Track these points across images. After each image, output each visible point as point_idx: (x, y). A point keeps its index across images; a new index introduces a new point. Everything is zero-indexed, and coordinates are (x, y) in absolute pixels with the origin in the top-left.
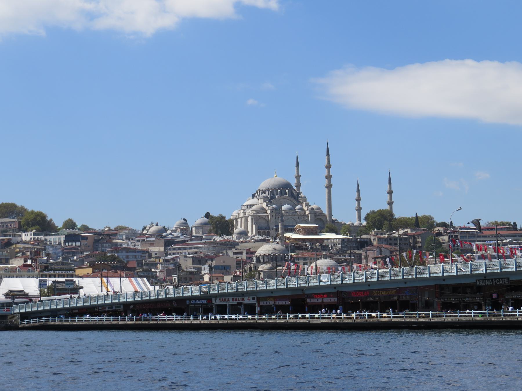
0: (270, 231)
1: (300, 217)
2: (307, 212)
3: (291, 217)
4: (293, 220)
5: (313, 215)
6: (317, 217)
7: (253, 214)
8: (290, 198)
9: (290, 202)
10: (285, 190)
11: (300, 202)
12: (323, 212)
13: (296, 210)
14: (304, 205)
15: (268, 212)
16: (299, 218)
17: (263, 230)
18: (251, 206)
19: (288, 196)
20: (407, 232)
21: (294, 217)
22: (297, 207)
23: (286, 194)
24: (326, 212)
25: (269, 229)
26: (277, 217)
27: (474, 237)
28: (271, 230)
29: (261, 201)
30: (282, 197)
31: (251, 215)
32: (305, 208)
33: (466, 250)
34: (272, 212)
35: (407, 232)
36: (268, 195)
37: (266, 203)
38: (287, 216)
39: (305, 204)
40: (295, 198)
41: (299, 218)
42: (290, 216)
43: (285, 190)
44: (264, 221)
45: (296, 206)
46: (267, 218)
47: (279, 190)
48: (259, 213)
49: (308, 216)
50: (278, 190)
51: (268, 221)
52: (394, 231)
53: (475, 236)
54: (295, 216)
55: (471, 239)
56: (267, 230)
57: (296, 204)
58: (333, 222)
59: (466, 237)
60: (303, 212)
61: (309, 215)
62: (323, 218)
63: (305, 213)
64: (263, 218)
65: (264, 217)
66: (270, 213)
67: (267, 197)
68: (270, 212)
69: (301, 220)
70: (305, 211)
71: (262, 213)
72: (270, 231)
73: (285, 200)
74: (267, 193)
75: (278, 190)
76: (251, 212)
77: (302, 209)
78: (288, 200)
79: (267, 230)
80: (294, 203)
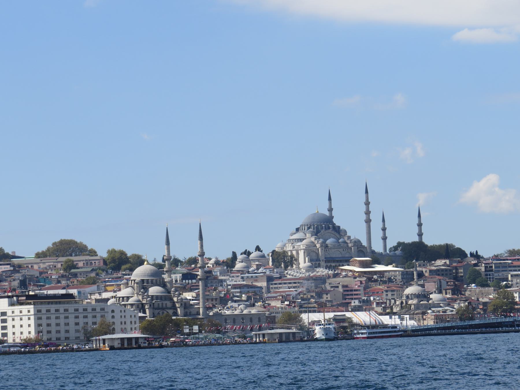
0: (320, 262)
1: (344, 250)
2: (350, 245)
3: (337, 249)
4: (340, 252)
5: (356, 247)
6: (359, 249)
7: (304, 248)
8: (333, 232)
9: (333, 235)
10: (328, 225)
11: (342, 235)
12: (363, 245)
13: (339, 243)
14: (346, 238)
15: (318, 246)
16: (343, 250)
17: (315, 262)
18: (301, 240)
19: (332, 230)
20: (446, 262)
21: (340, 250)
22: (340, 240)
23: (329, 228)
24: (365, 243)
25: (320, 261)
26: (325, 250)
27: (506, 267)
28: (322, 261)
29: (308, 235)
30: (327, 231)
31: (303, 249)
32: (349, 242)
33: (500, 278)
34: (321, 246)
35: (446, 262)
36: (314, 229)
37: (315, 237)
38: (334, 249)
39: (347, 237)
40: (337, 233)
41: (343, 250)
42: (336, 248)
43: (328, 225)
44: (315, 254)
45: (339, 240)
46: (317, 251)
47: (323, 225)
48: (310, 247)
49: (351, 249)
50: (322, 225)
51: (318, 254)
52: (433, 262)
53: (507, 267)
54: (340, 248)
55: (503, 269)
56: (318, 262)
57: (338, 237)
58: (372, 253)
59: (499, 267)
60: (346, 245)
61: (353, 248)
62: (363, 250)
63: (348, 246)
64: (313, 251)
65: (315, 250)
66: (321, 247)
67: (313, 232)
68: (320, 246)
69: (345, 252)
70: (347, 243)
71: (312, 247)
72: (320, 262)
73: (329, 234)
74: (312, 228)
75: (322, 225)
76: (301, 246)
77: (345, 242)
78: (331, 234)
79: (318, 262)
80: (336, 236)
